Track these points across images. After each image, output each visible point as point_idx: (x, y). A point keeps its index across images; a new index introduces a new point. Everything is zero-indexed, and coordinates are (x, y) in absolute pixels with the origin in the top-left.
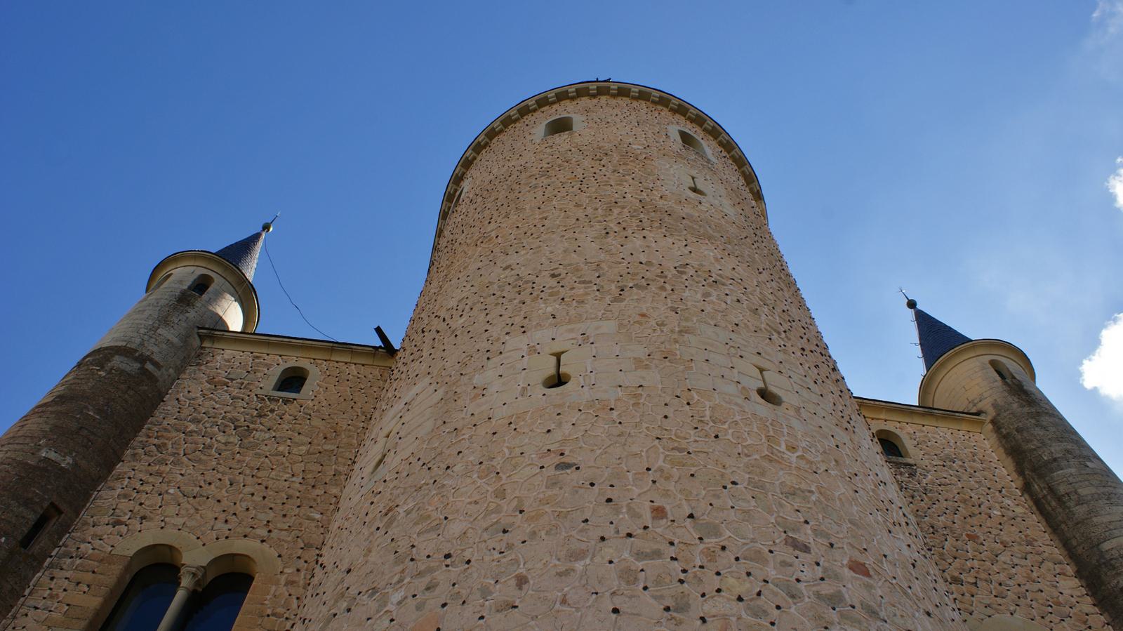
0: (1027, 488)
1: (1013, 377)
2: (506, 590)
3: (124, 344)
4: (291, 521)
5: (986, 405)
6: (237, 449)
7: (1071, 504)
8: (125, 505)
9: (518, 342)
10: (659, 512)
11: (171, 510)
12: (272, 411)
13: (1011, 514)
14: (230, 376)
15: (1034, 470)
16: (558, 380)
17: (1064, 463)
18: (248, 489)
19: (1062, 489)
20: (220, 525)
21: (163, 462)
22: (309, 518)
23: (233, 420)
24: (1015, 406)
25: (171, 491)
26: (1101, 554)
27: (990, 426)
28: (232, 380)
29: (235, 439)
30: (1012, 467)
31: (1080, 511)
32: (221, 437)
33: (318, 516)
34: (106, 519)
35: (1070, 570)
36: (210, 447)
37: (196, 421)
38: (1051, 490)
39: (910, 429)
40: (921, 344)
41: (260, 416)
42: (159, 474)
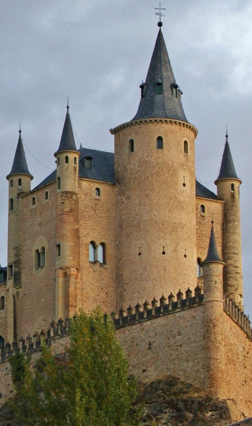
0: (223, 224)
1: (234, 191)
2: (160, 286)
3: (72, 191)
4: (108, 235)
5: (225, 198)
6: (95, 216)
7: (228, 233)
8: (84, 232)
9: (158, 241)
10: (173, 278)
11: (91, 233)
12: (97, 204)
13: (217, 230)
14: (87, 192)
15: (226, 221)
16: (164, 253)
17: (231, 222)
18: (100, 227)
19: (228, 229)
20: (98, 236)
21: (85, 221)
22: (110, 234)
23: (92, 207)
24: (230, 202)
25: (89, 228)
26: (227, 245)
27: (223, 204)
28: (88, 193)
29: (94, 213)
30: (223, 217)
31: (228, 235)
32: (92, 213)
33: (111, 233)
34: (83, 236)
35: (221, 245)
36: (91, 216)
37: (86, 208)
38: (226, 228)
39: (208, 204)
40: (223, 156)
41: (96, 205)
42: (86, 224)
